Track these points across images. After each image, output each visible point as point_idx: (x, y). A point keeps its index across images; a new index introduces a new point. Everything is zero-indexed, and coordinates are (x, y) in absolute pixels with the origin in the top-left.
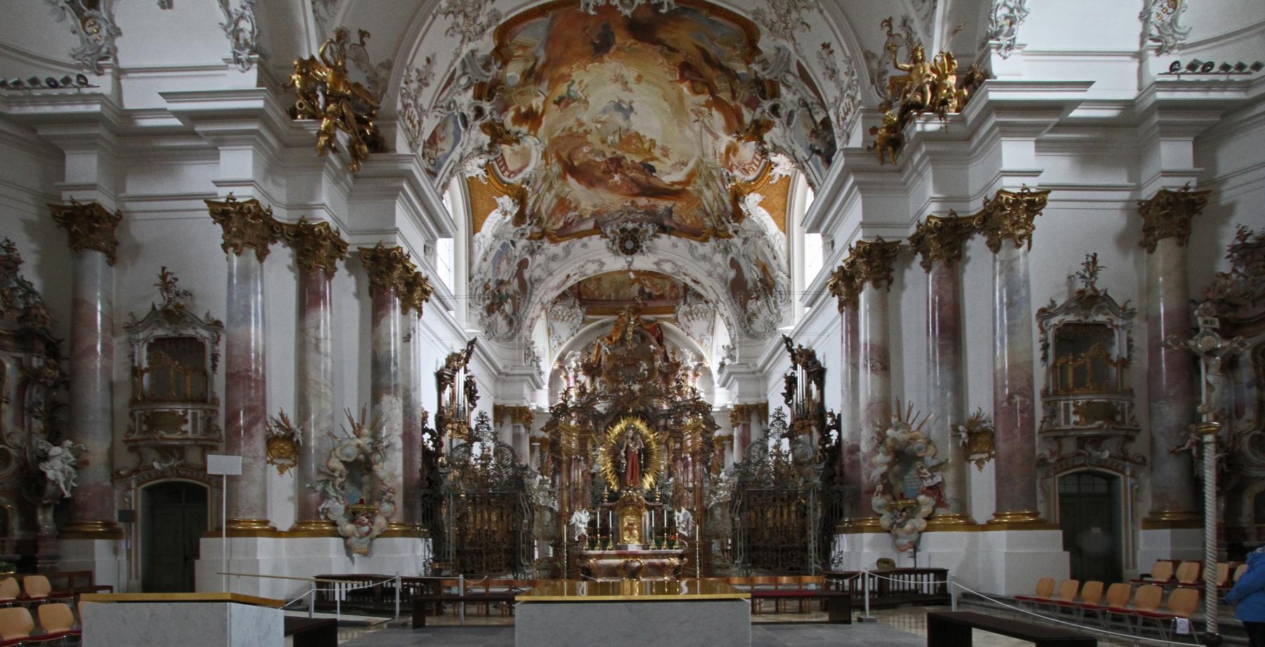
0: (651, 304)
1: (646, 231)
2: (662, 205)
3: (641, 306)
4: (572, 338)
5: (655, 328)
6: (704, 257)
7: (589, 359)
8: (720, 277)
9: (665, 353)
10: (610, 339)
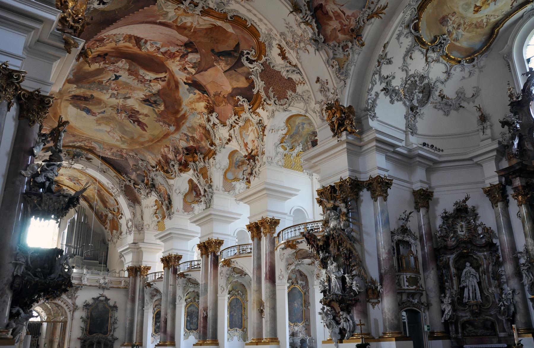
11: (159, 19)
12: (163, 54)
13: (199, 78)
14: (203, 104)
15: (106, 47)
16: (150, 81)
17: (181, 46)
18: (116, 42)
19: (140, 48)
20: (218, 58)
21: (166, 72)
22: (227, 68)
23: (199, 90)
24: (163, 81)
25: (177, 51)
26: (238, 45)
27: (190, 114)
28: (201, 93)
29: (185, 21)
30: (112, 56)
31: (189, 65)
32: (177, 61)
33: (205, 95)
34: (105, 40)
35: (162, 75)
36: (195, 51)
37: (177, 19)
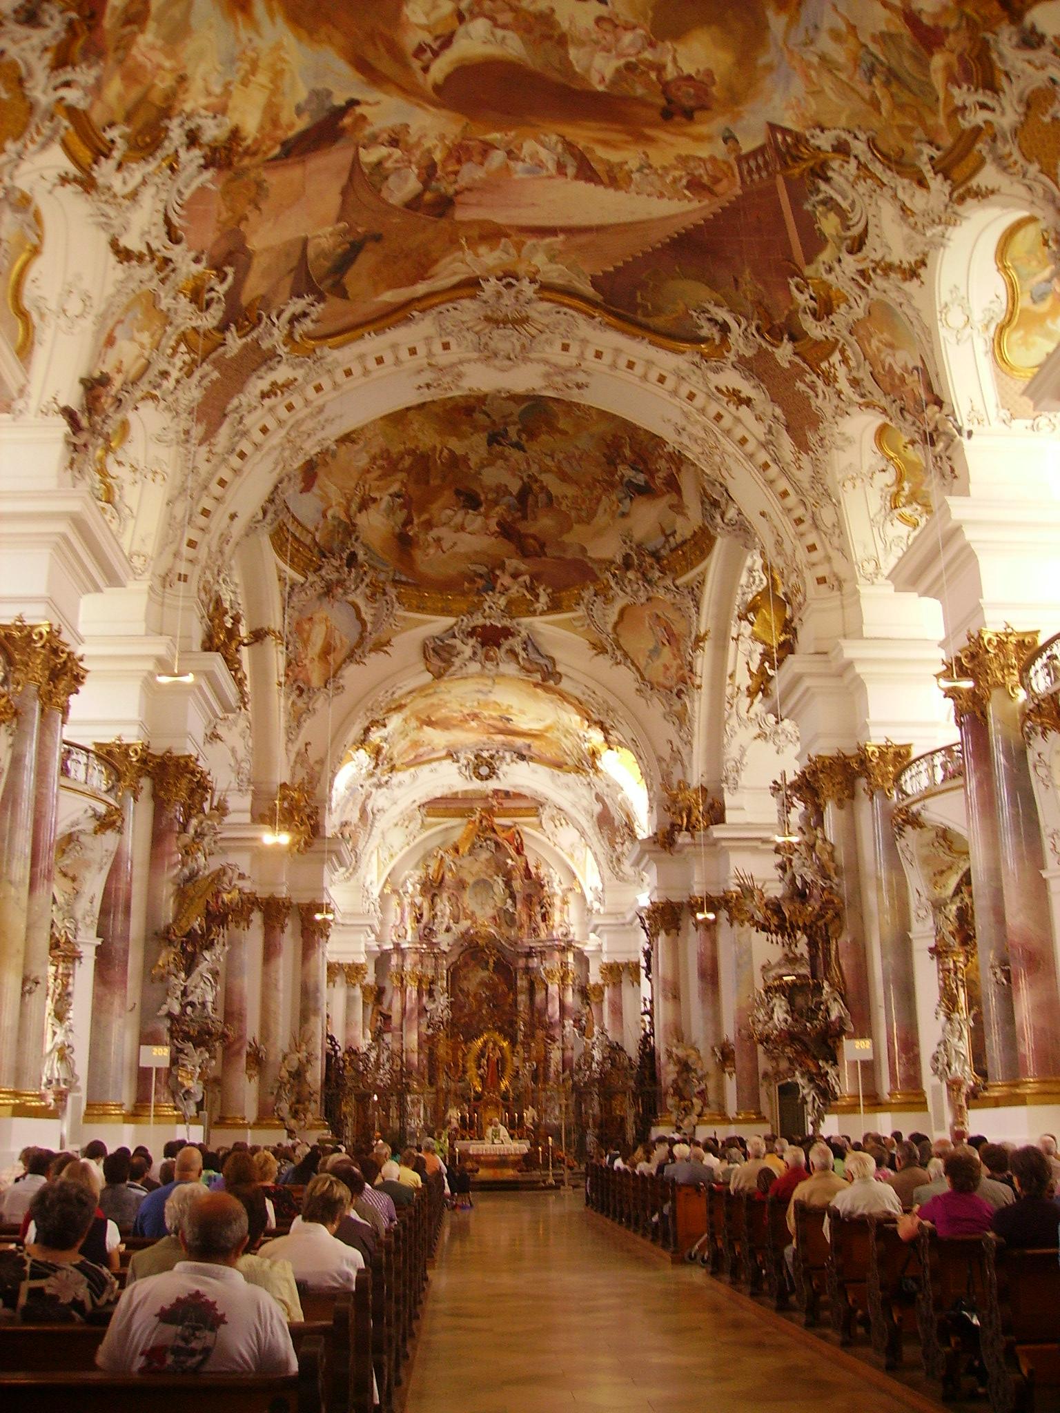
0: (508, 804)
1: (504, 758)
2: (519, 742)
3: (496, 809)
4: (407, 848)
5: (513, 834)
6: (567, 786)
7: (428, 875)
8: (587, 811)
9: (527, 869)
10: (457, 850)
11: (564, 243)
12: (487, 148)
13: (336, 159)
14: (251, 124)
15: (675, 151)
16: (461, 18)
17: (457, 193)
18: (650, 167)
19: (569, 147)
20: (350, 238)
21: (437, 88)
22: (311, 252)
23: (304, 136)
24: (420, 50)
25: (456, 173)
26: (343, 293)
27: (238, 39)
28: (291, 134)
29: (497, 253)
30: (640, 101)
31: (397, 161)
32: (436, 147)
33: (277, 151)
34: (684, 182)
35: (440, 68)
36: (413, 204)
37: (519, 251)
